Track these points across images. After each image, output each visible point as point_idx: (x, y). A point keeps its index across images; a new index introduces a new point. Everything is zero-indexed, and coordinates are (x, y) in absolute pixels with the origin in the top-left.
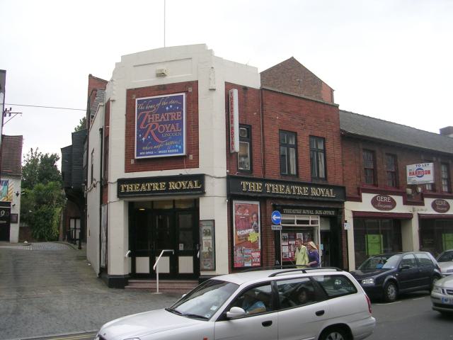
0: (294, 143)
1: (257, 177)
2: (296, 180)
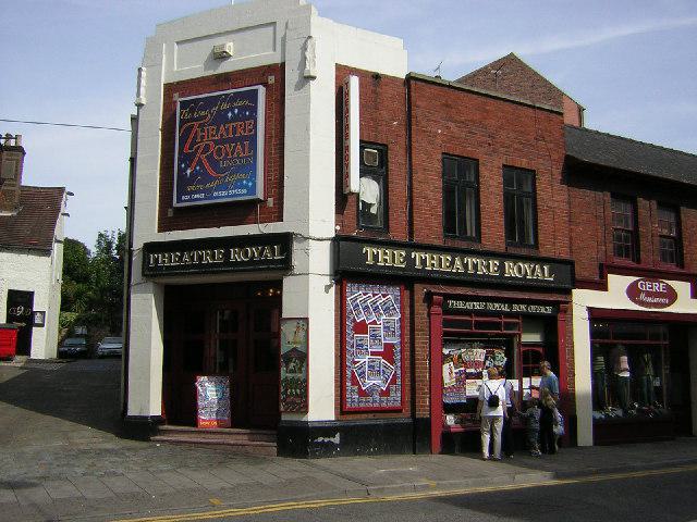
0: (530, 190)
1: (492, 248)
2: (533, 253)
